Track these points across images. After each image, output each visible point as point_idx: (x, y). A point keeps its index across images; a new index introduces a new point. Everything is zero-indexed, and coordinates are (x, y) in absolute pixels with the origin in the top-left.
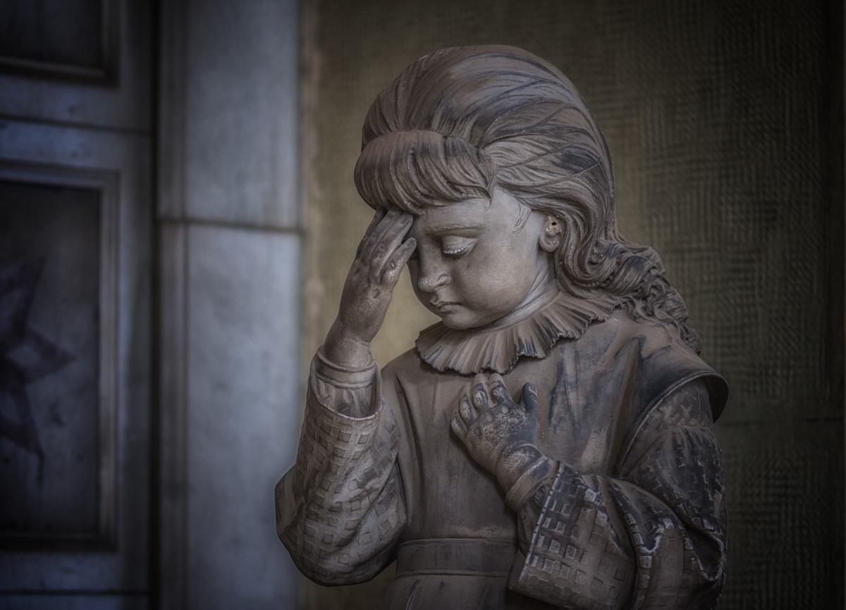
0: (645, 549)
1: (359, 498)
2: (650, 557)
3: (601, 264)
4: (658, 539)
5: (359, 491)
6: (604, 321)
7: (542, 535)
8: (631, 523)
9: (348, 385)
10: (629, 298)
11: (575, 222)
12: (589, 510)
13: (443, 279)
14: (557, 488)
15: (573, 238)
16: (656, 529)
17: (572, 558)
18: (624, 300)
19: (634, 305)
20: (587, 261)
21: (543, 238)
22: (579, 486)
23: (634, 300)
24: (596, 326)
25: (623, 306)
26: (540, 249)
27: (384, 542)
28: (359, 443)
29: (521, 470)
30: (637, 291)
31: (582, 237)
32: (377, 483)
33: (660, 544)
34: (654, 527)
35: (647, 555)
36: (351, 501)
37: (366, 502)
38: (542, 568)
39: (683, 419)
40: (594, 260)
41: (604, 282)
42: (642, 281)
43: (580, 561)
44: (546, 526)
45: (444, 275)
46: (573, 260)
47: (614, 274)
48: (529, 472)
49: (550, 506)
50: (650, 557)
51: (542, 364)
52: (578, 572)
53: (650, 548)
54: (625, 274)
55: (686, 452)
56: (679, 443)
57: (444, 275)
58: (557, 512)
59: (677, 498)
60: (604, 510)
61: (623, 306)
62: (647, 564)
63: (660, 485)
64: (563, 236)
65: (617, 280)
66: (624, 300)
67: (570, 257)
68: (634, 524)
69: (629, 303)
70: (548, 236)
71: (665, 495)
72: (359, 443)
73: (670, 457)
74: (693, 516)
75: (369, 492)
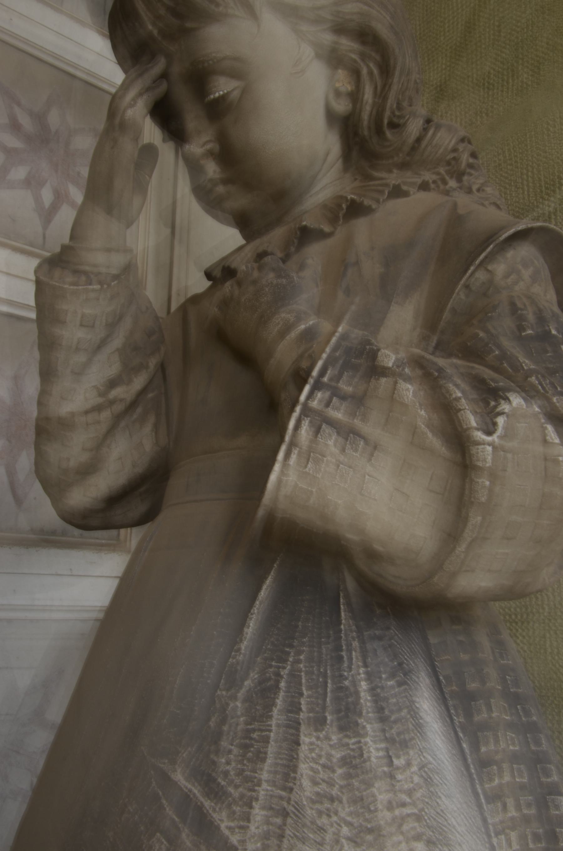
0: (479, 435)
1: (98, 409)
2: (489, 449)
3: (405, 124)
4: (501, 421)
5: (100, 400)
6: (406, 194)
7: (307, 416)
8: (454, 396)
9: (87, 268)
10: (438, 174)
11: (371, 73)
12: (383, 380)
13: (209, 146)
14: (334, 350)
15: (368, 95)
16: (495, 407)
17: (358, 455)
18: (434, 177)
19: (445, 182)
20: (386, 121)
21: (331, 96)
22: (368, 347)
23: (447, 178)
24: (400, 202)
25: (432, 186)
26: (331, 116)
27: (139, 470)
28: (81, 325)
29: (283, 334)
30: (448, 163)
31: (379, 88)
32: (124, 393)
33: (505, 428)
34: (493, 403)
35: (484, 444)
36: (87, 412)
37: (106, 415)
38: (306, 467)
39: (521, 284)
40: (395, 120)
41: (408, 154)
42: (455, 150)
43: (370, 460)
44: (314, 404)
45: (210, 141)
46: (369, 128)
47: (419, 140)
48: (293, 334)
49: (322, 373)
50: (489, 449)
51: (329, 242)
52: (367, 477)
53: (489, 433)
54: (434, 134)
55: (531, 317)
56: (519, 305)
57: (210, 141)
58: (333, 384)
59: (525, 368)
60: (407, 379)
61: (432, 186)
62: (485, 460)
63: (497, 353)
64: (355, 97)
65: (424, 143)
66: (434, 177)
67: (365, 123)
68: (460, 398)
69: (439, 182)
70: (338, 94)
71: (505, 365)
72: (81, 325)
73: (508, 323)
74: (554, 395)
75: (112, 403)
